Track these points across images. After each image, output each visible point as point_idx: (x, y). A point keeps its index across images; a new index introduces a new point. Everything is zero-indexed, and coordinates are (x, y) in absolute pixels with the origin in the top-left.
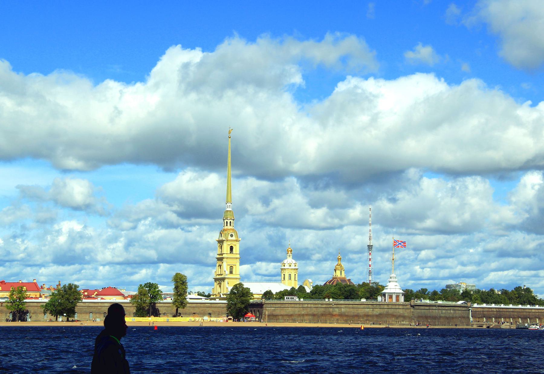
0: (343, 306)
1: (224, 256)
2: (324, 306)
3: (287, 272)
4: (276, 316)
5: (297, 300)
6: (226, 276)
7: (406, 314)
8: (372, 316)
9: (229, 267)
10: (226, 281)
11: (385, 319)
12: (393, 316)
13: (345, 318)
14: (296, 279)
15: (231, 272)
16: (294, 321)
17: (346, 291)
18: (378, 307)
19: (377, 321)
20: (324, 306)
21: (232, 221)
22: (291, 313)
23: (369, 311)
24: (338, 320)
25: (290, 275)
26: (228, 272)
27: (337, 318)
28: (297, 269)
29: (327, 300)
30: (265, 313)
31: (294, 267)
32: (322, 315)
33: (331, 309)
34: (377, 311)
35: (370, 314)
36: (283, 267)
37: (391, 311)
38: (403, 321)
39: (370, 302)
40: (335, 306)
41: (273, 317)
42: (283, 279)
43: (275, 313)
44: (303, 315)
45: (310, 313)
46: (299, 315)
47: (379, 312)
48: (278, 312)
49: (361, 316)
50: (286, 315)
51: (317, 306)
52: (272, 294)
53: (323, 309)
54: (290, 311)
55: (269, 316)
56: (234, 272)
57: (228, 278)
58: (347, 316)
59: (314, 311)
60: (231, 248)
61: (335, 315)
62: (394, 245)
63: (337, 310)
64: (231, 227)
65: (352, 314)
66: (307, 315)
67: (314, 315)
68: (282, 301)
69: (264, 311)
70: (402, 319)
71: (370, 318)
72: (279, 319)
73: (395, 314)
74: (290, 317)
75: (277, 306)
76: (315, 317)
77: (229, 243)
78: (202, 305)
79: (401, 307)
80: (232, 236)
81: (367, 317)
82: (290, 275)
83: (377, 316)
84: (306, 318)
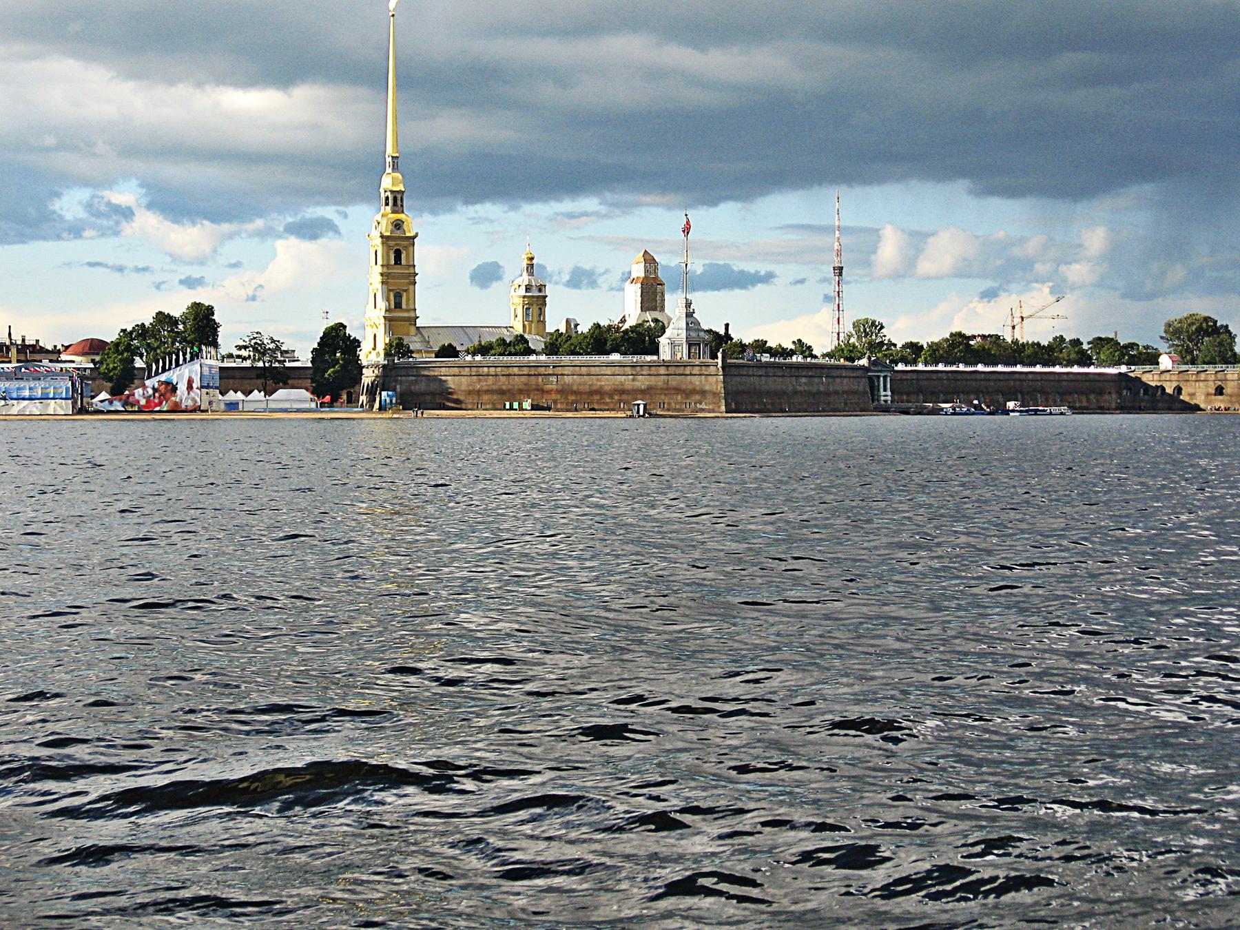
0: (567, 371)
7: (707, 388)
9: (392, 295)
12: (678, 390)
13: (571, 398)
20: (525, 371)
27: (554, 396)
37: (673, 382)
43: (415, 388)
44: (479, 392)
49: (606, 393)
53: (523, 379)
56: (404, 306)
61: (549, 392)
63: (554, 379)
65: (587, 388)
66: (487, 392)
67: (501, 392)
70: (698, 397)
71: (625, 397)
73: (684, 387)
77: (392, 243)
84: (486, 398)
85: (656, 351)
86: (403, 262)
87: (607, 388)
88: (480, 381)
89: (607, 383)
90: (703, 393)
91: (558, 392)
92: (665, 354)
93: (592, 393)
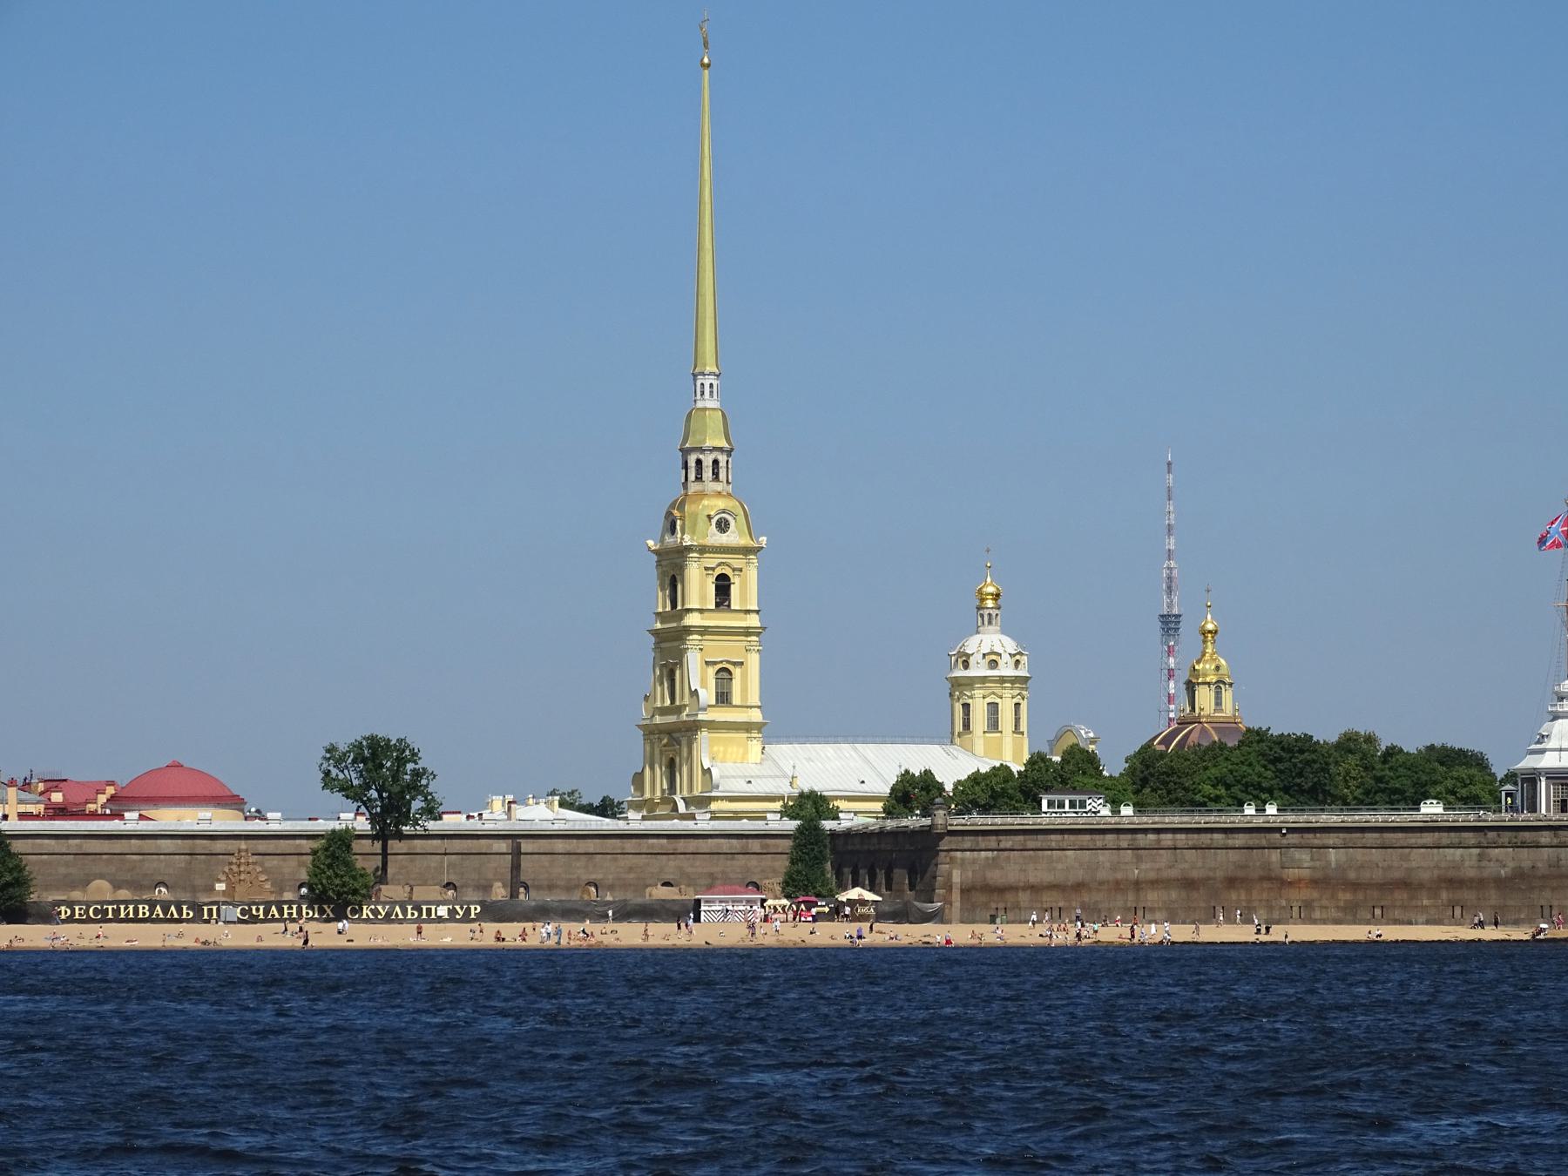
0: (1331, 839)
1: (692, 620)
2: (1240, 840)
3: (978, 693)
4: (1001, 890)
5: (1106, 811)
6: (700, 717)
8: (1479, 884)
9: (711, 671)
10: (703, 735)
11: (1545, 897)
13: (1345, 897)
14: (1024, 727)
15: (723, 698)
17: (1293, 769)
18: (1506, 837)
19: (1503, 908)
21: (722, 459)
22: (1079, 875)
23: (1464, 859)
24: (1308, 905)
25: (993, 707)
26: (708, 695)
28: (1024, 680)
29: (1250, 810)
30: (950, 875)
32: (1231, 882)
33: (1275, 856)
34: (1505, 860)
35: (1472, 873)
36: (960, 673)
39: (1465, 817)
40: (1293, 839)
41: (988, 898)
42: (959, 727)
43: (995, 877)
44: (1137, 885)
45: (1174, 873)
46: (1118, 887)
48: (1012, 870)
49: (1421, 886)
51: (1205, 839)
52: (940, 787)
54: (1069, 863)
55: (966, 891)
56: (736, 700)
57: (713, 726)
58: (1355, 886)
59: (1192, 863)
60: (723, 587)
63: (1304, 856)
64: (718, 487)
65: (1378, 876)
66: (1154, 883)
67: (1189, 884)
68: (1027, 820)
69: (943, 868)
71: (1469, 896)
72: (1017, 907)
75: (1007, 842)
76: (1198, 894)
78: (630, 845)
80: (723, 526)
81: (1454, 892)
82: (993, 707)
83: (1500, 883)
84: (1152, 897)
87: (1425, 876)
88: (1139, 859)
89: (1422, 862)
91: (1314, 883)
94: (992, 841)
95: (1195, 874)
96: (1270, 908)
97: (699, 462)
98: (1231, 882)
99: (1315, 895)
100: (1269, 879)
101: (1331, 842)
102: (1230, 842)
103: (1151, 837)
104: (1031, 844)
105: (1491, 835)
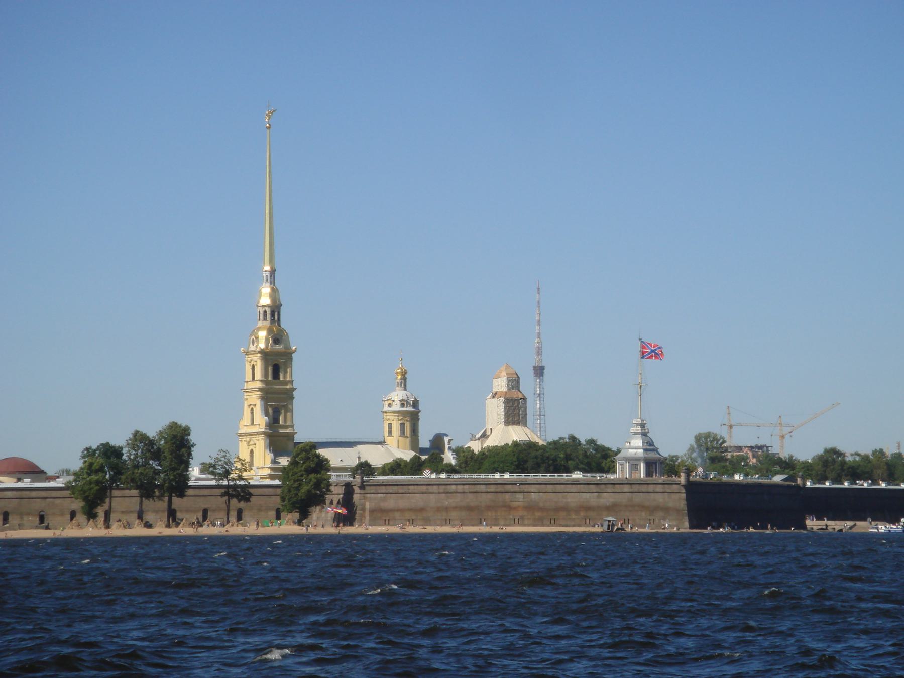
0: (533, 488)
7: (671, 505)
12: (643, 507)
13: (538, 514)
16: (427, 522)
23: (590, 498)
24: (522, 518)
27: (521, 513)
29: (497, 476)
31: (410, 409)
32: (489, 508)
33: (507, 496)
34: (607, 499)
37: (638, 498)
38: (664, 519)
43: (384, 505)
44: (447, 509)
46: (438, 509)
47: (611, 500)
48: (391, 502)
50: (410, 510)
51: (478, 488)
53: (489, 496)
55: (372, 511)
58: (542, 509)
61: (515, 508)
62: (643, 353)
63: (520, 496)
66: (455, 508)
67: (469, 509)
70: (661, 514)
71: (591, 514)
74: (419, 513)
76: (475, 513)
79: (659, 488)
84: (454, 514)
85: (611, 469)
86: (281, 378)
89: (573, 499)
90: (666, 510)
92: (623, 471)
93: (558, 510)
94: (383, 489)
95: (472, 504)
96: (506, 519)
97: (265, 312)
98: (489, 508)
99: (525, 513)
100: (505, 506)
101: (533, 490)
102: (489, 490)
103: (453, 487)
104: (400, 491)
105: (603, 486)
